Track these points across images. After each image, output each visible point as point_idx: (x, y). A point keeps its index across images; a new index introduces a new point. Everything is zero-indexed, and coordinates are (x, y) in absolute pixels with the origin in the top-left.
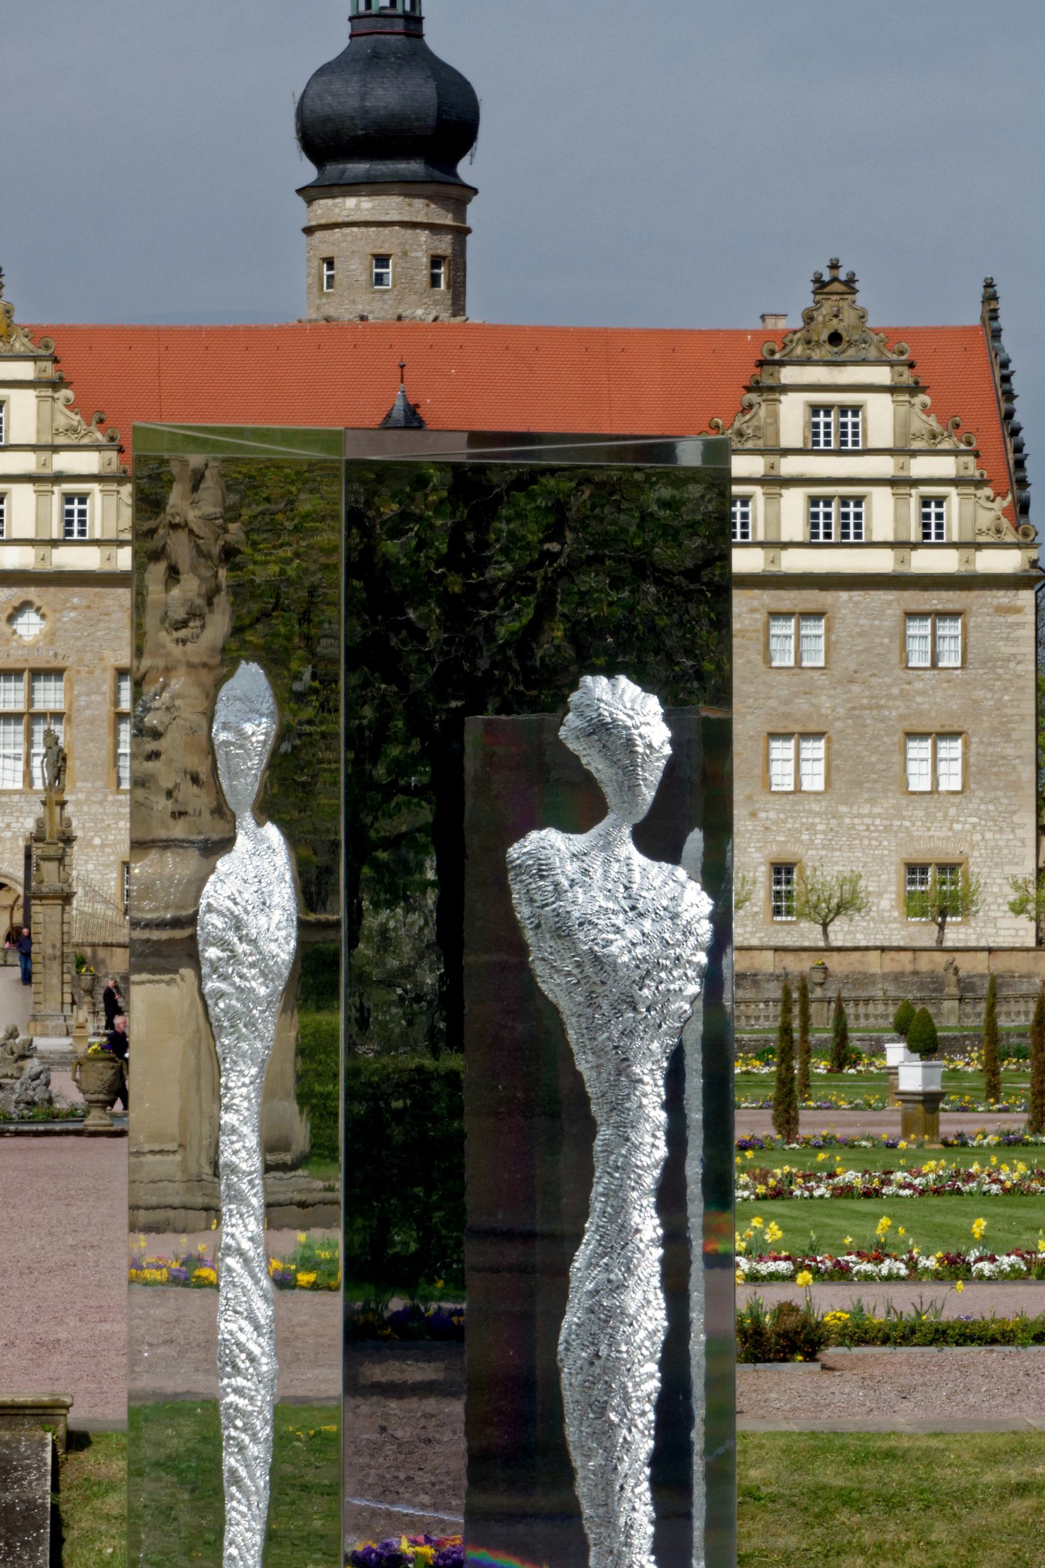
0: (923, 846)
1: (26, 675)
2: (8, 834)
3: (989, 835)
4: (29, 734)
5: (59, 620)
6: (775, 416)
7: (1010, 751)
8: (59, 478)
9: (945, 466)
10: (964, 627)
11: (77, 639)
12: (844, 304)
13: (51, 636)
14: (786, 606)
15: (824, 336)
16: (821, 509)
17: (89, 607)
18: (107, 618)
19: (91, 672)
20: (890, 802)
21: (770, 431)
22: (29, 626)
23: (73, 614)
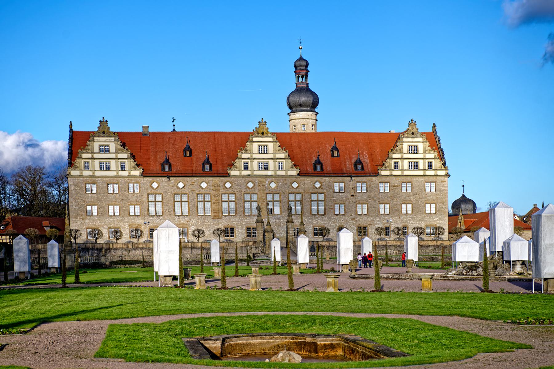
0: (429, 223)
3: (440, 221)
6: (402, 147)
7: (444, 206)
8: (278, 159)
9: (432, 156)
10: (435, 185)
12: (414, 127)
13: (277, 187)
15: (411, 133)
16: (411, 164)
20: (423, 215)
21: (401, 150)
22: (273, 185)
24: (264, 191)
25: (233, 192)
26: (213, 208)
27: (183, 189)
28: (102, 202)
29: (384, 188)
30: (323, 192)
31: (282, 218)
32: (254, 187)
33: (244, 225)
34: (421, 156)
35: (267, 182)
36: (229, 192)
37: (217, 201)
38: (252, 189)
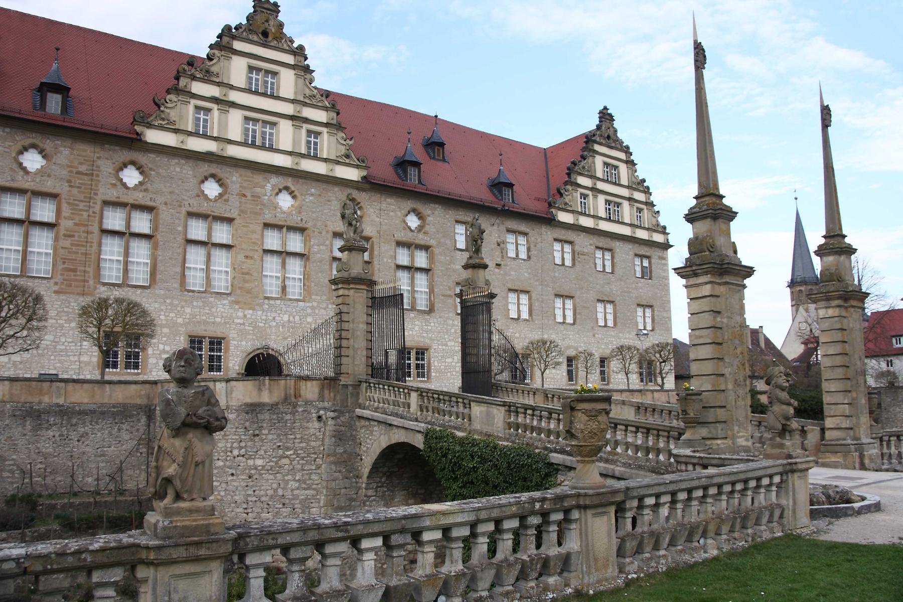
1: (285, 229)
2: (274, 324)
5: (304, 200)
6: (594, 163)
8: (306, 120)
11: (314, 212)
13: (300, 209)
14: (601, 245)
17: (320, 195)
18: (329, 203)
19: (320, 233)
21: (593, 169)
23: (311, 198)
24: (256, 213)
26: (61, 251)
29: (560, 253)
30: (427, 244)
31: (309, 311)
32: (226, 197)
33: (181, 325)
34: (625, 192)
35: (269, 187)
36: (133, 202)
37: (82, 229)
38: (218, 204)
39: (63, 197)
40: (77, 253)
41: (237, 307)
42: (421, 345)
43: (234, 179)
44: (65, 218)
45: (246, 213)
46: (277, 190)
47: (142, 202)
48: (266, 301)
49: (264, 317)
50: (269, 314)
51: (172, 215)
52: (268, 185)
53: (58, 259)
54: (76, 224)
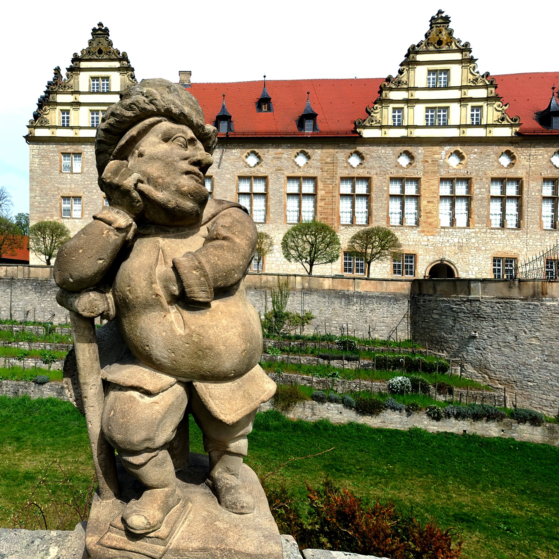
2: (448, 244)
4: (453, 206)
24: (435, 172)
25: (368, 175)
27: (258, 167)
28: (92, 192)
36: (356, 175)
37: (330, 195)
39: (319, 178)
40: (328, 209)
41: (423, 234)
42: (509, 256)
43: (420, 151)
44: (321, 190)
45: (427, 173)
46: (450, 154)
47: (363, 175)
48: (443, 230)
49: (441, 240)
50: (445, 238)
51: (381, 181)
52: (443, 151)
53: (318, 213)
54: (326, 193)
